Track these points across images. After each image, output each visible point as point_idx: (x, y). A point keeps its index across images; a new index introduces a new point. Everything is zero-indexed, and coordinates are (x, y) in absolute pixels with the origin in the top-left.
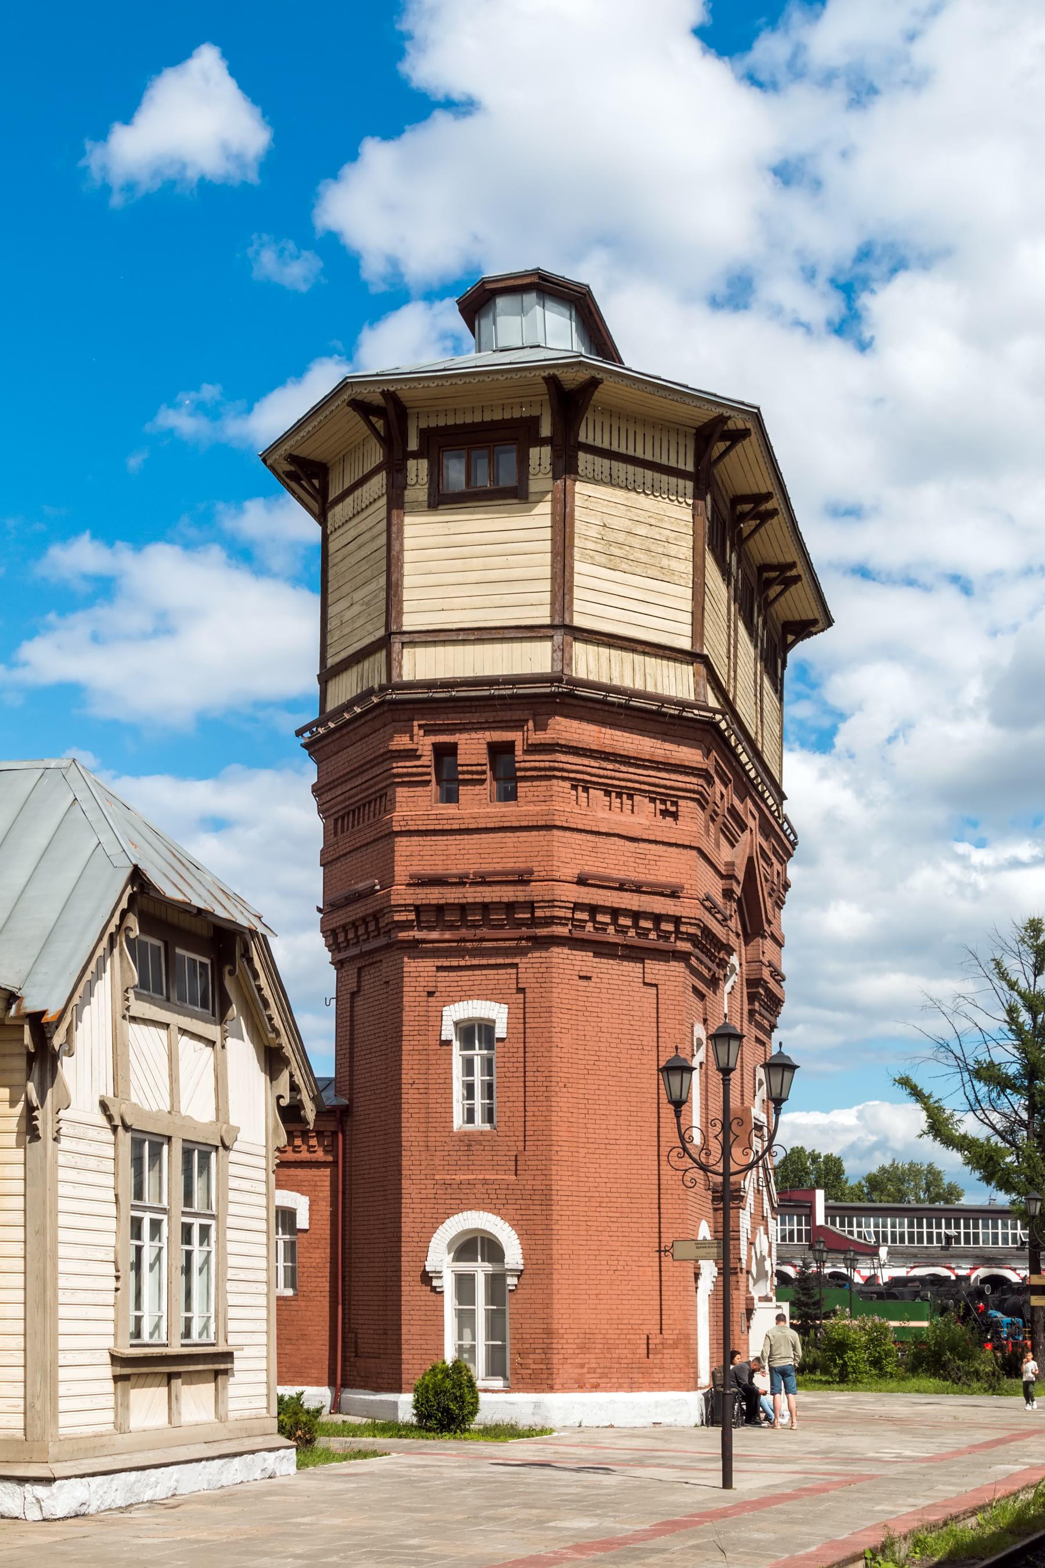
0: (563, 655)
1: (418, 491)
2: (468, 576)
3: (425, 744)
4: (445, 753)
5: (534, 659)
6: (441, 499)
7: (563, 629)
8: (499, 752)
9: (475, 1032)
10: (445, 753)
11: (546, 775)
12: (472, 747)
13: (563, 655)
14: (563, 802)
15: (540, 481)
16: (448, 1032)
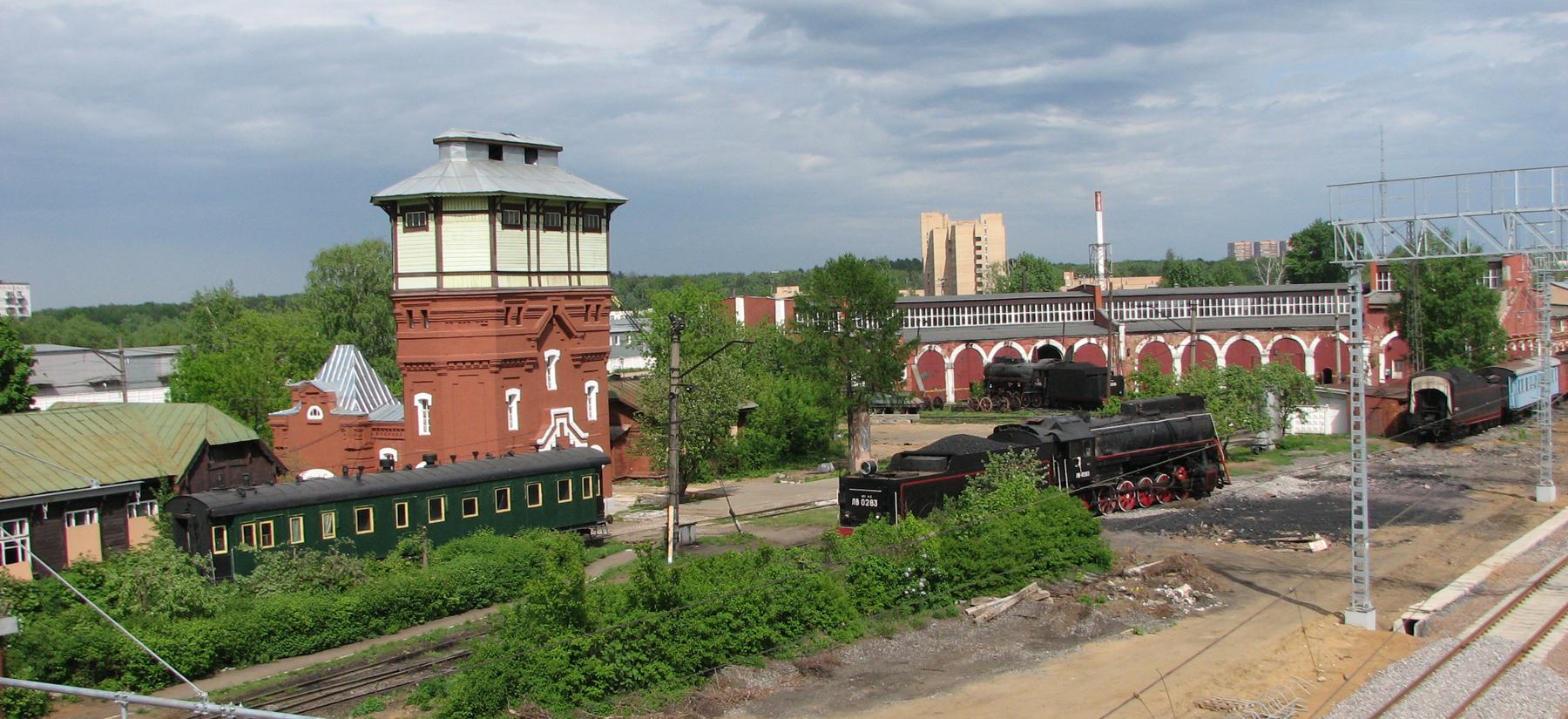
0: (440, 283)
1: (400, 227)
2: (414, 253)
3: (404, 311)
4: (410, 313)
5: (431, 283)
6: (406, 230)
7: (440, 273)
8: (424, 313)
9: (424, 402)
10: (410, 313)
11: (435, 321)
12: (417, 313)
13: (440, 283)
14: (443, 330)
15: (432, 225)
16: (417, 403)
